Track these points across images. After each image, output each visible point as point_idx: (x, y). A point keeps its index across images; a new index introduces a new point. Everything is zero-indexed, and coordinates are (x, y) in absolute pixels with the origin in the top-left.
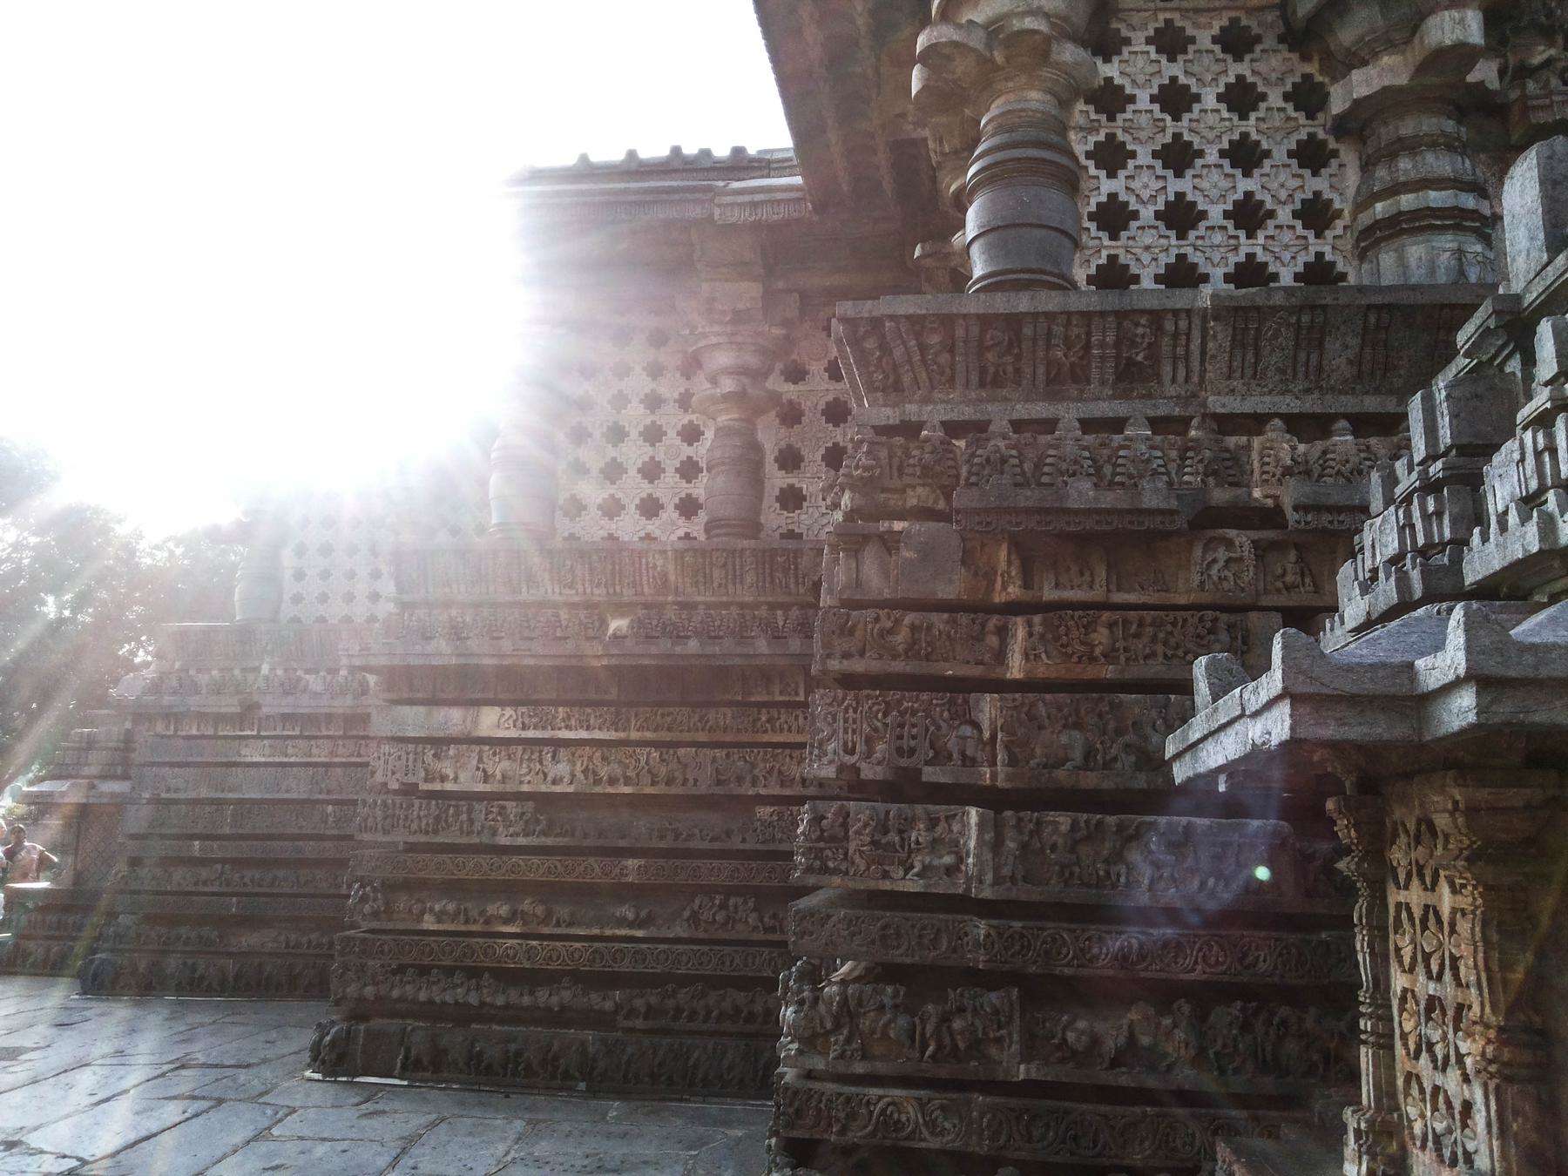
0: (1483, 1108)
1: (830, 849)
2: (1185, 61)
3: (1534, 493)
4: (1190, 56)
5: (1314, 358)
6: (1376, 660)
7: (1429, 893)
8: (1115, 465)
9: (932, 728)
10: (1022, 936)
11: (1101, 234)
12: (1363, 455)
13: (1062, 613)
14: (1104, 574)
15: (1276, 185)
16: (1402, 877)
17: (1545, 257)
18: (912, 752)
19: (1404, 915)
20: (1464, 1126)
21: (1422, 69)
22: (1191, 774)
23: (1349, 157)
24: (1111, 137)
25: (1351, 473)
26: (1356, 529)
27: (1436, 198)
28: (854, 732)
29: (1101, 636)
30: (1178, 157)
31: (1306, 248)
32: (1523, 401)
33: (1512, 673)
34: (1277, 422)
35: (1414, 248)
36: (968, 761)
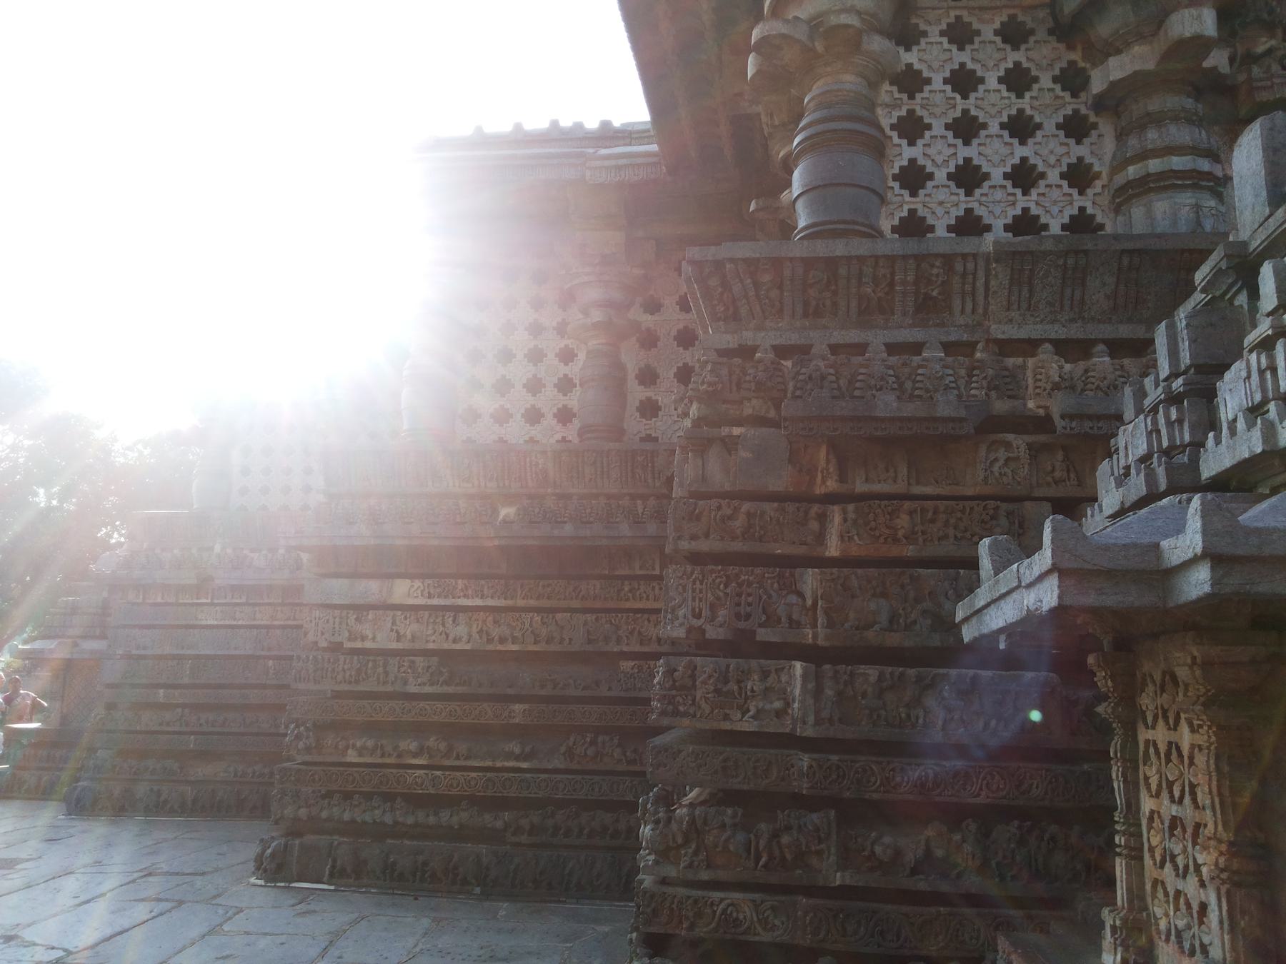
0: (1216, 908)
1: (681, 695)
2: (972, 50)
3: (1257, 405)
4: (976, 46)
5: (1078, 294)
6: (1128, 541)
7: (1172, 732)
8: (915, 382)
9: (765, 597)
10: (838, 767)
11: (903, 192)
12: (1118, 373)
13: (871, 502)
14: (905, 470)
15: (1046, 152)
16: (1150, 719)
17: (1267, 211)
18: (748, 616)
19: (1152, 750)
20: (1201, 923)
21: (1166, 56)
22: (976, 634)
23: (1106, 128)
24: (911, 112)
25: (1108, 388)
26: (1112, 433)
27: (1178, 163)
28: (700, 600)
29: (903, 521)
30: (966, 128)
31: (1071, 203)
32: (1249, 328)
33: (1240, 552)
34: (1048, 346)
35: (1160, 203)
36: (794, 624)
